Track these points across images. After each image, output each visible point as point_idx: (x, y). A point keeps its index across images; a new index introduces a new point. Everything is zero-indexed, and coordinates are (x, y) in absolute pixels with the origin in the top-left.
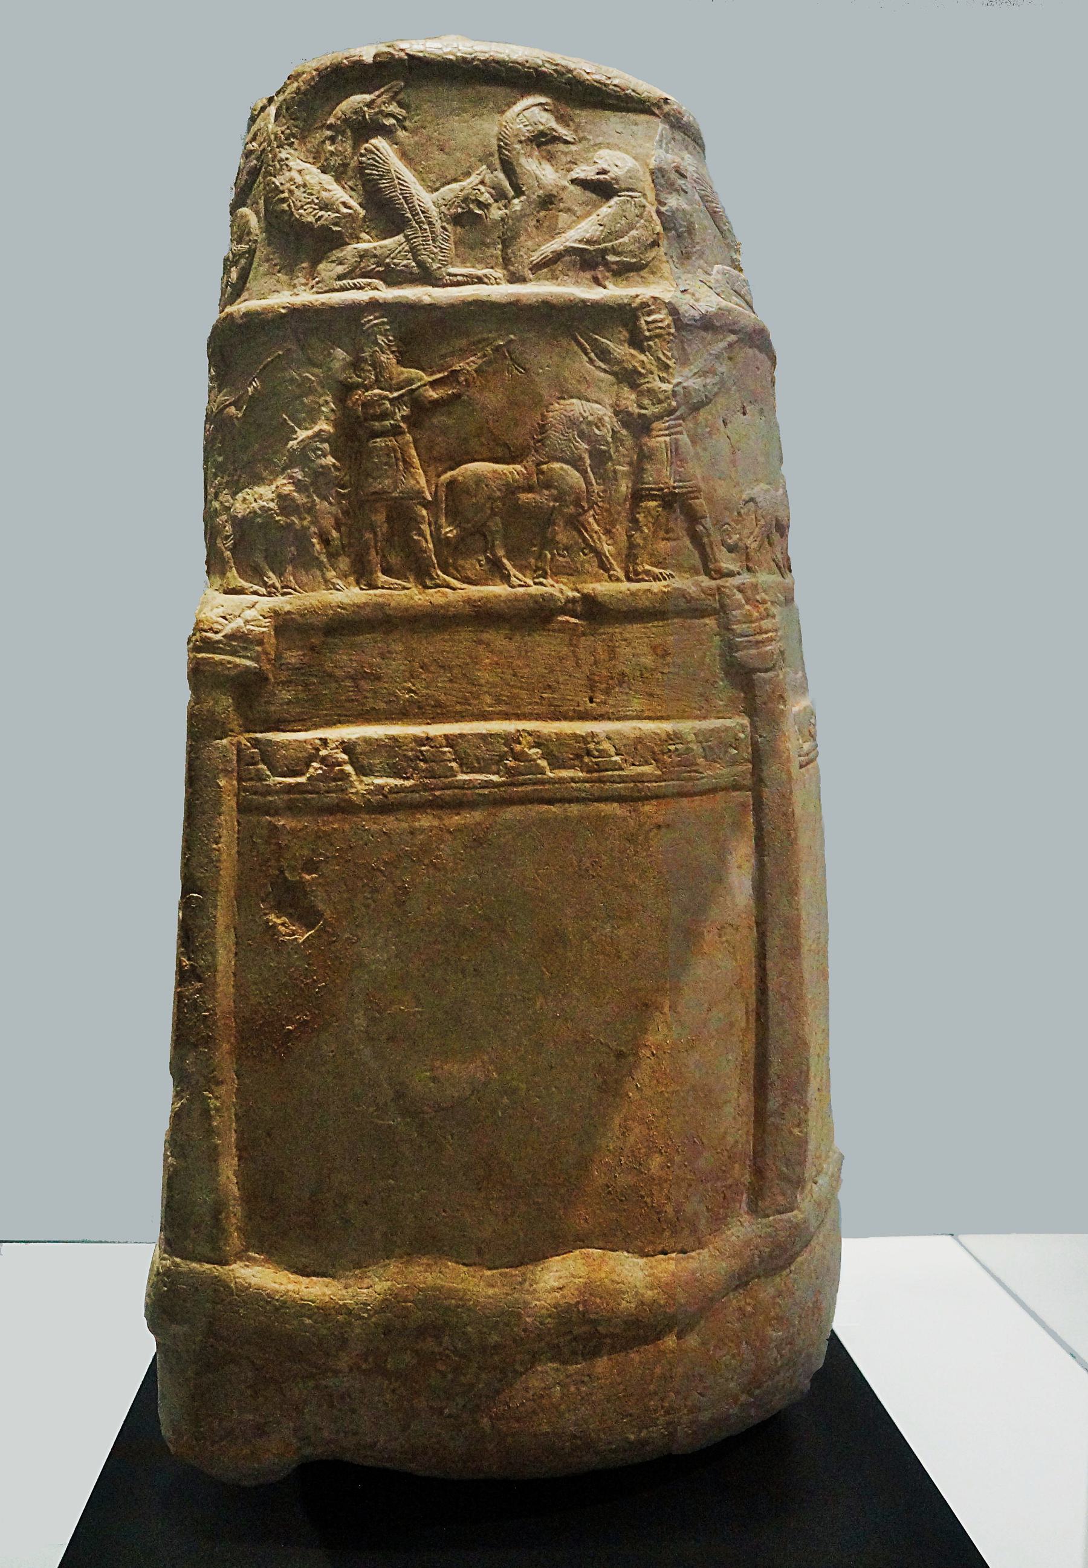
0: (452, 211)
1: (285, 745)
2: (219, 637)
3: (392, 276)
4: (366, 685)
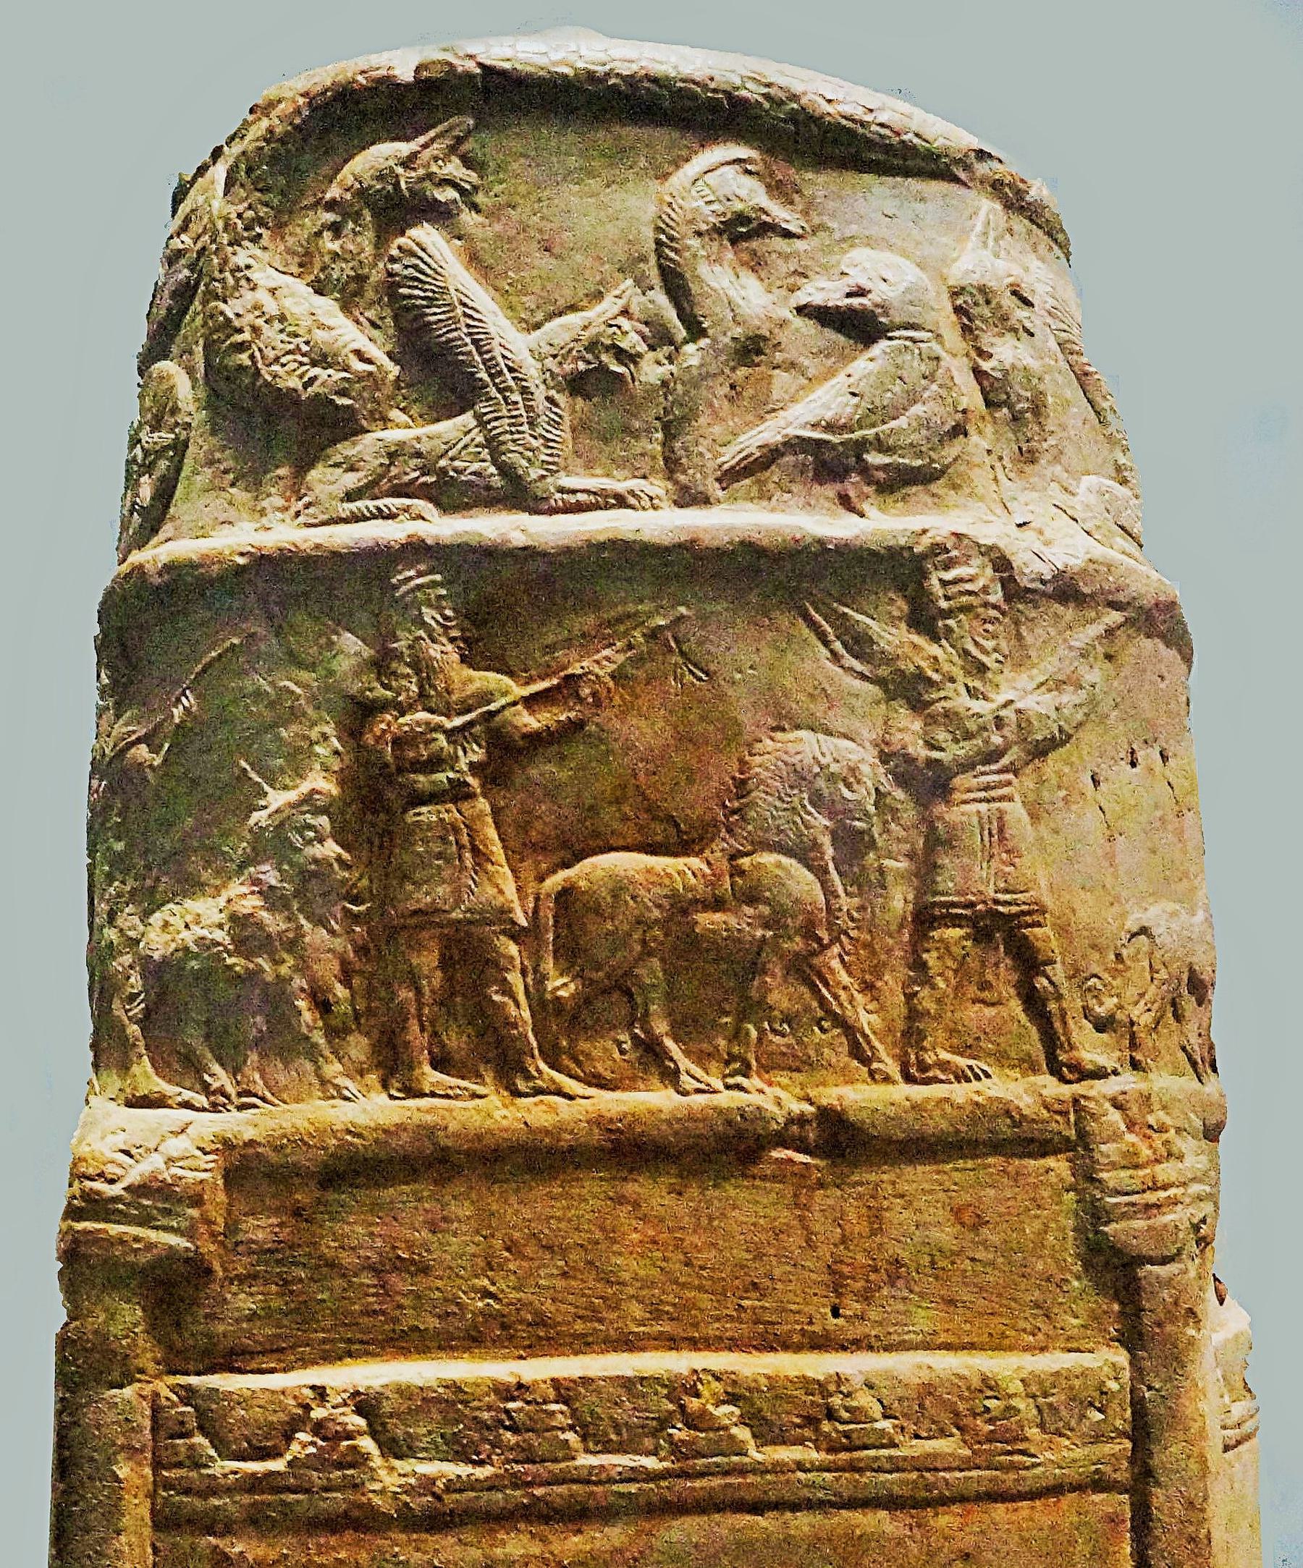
0: (568, 367)
3: (448, 493)
4: (401, 1283)
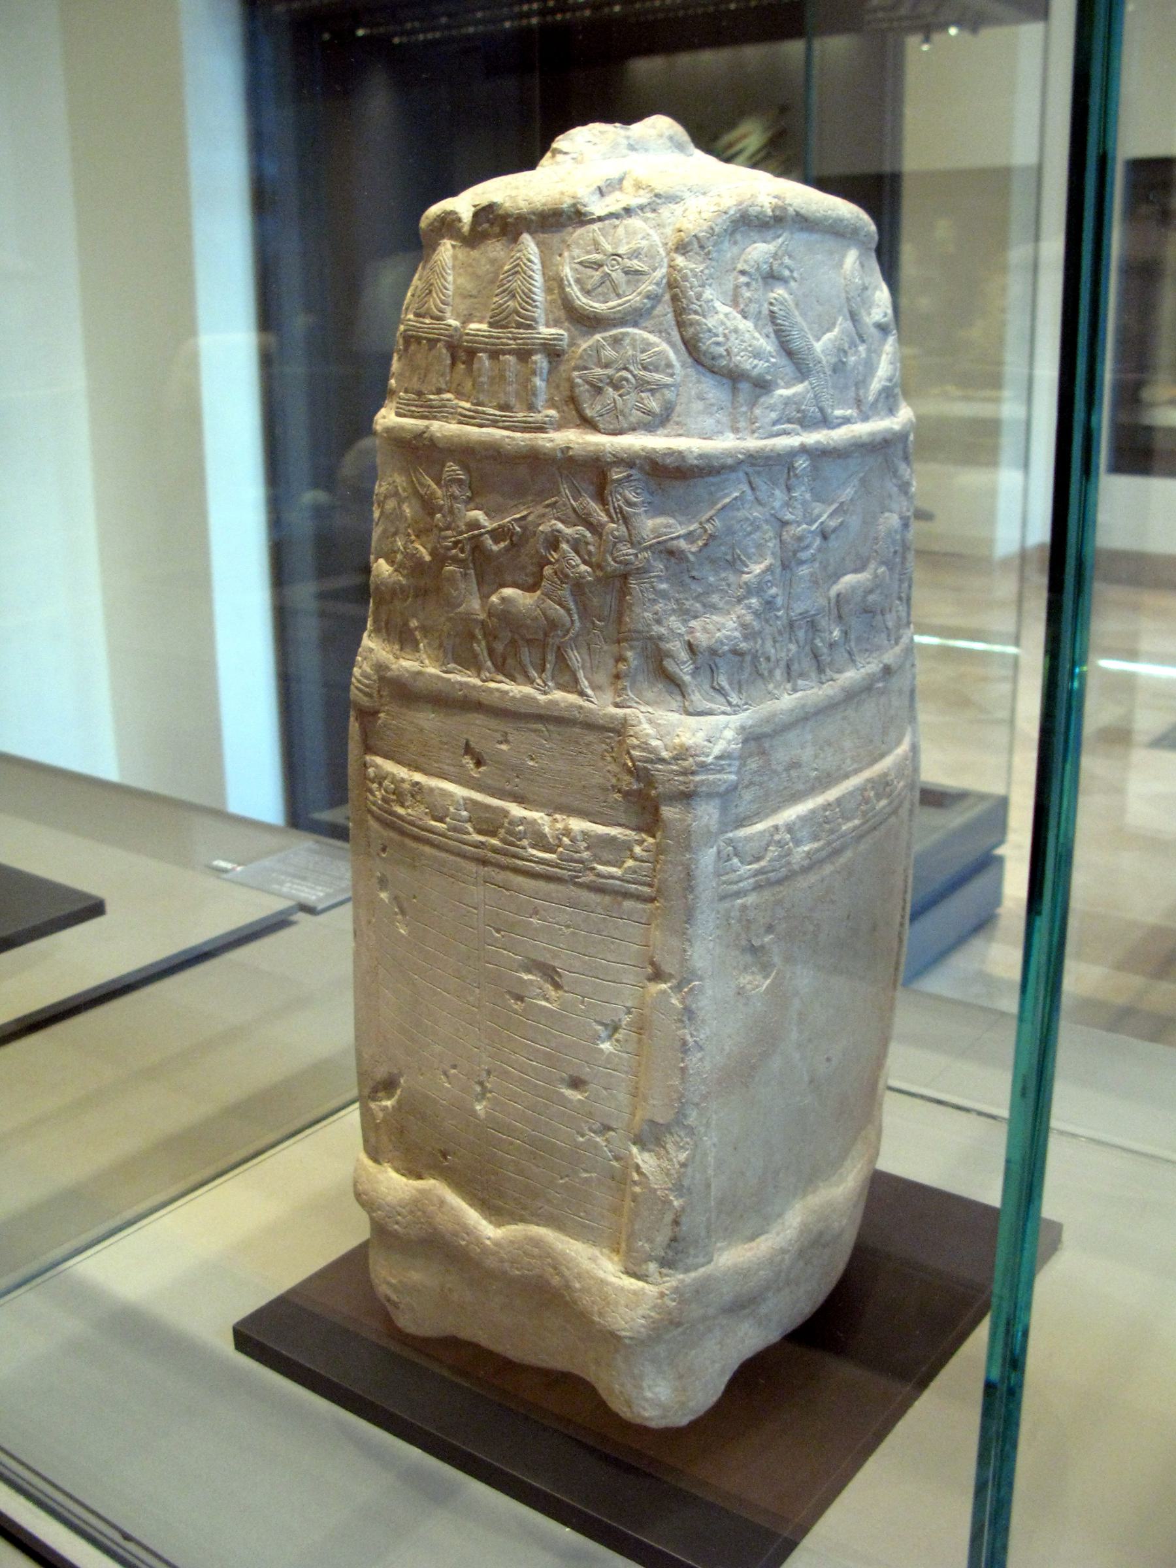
1: (749, 839)
2: (710, 759)
3: (806, 423)
4: (793, 773)
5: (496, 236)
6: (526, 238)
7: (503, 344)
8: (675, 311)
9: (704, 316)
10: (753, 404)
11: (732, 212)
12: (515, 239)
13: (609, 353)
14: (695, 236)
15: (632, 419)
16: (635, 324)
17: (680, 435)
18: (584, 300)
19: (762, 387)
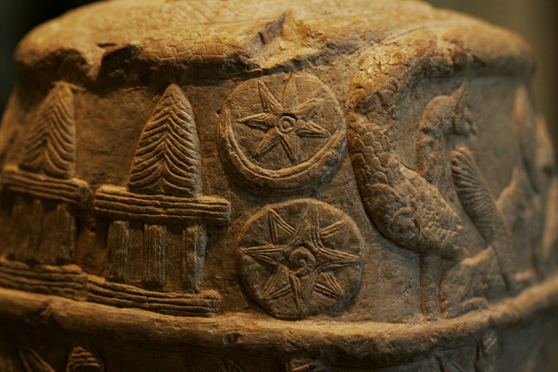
5: (132, 84)
6: (174, 89)
7: (148, 212)
8: (357, 179)
9: (391, 185)
10: (441, 278)
11: (413, 64)
12: (161, 90)
13: (283, 226)
14: (377, 93)
15: (313, 302)
16: (313, 194)
17: (367, 320)
18: (252, 166)
19: (450, 259)
